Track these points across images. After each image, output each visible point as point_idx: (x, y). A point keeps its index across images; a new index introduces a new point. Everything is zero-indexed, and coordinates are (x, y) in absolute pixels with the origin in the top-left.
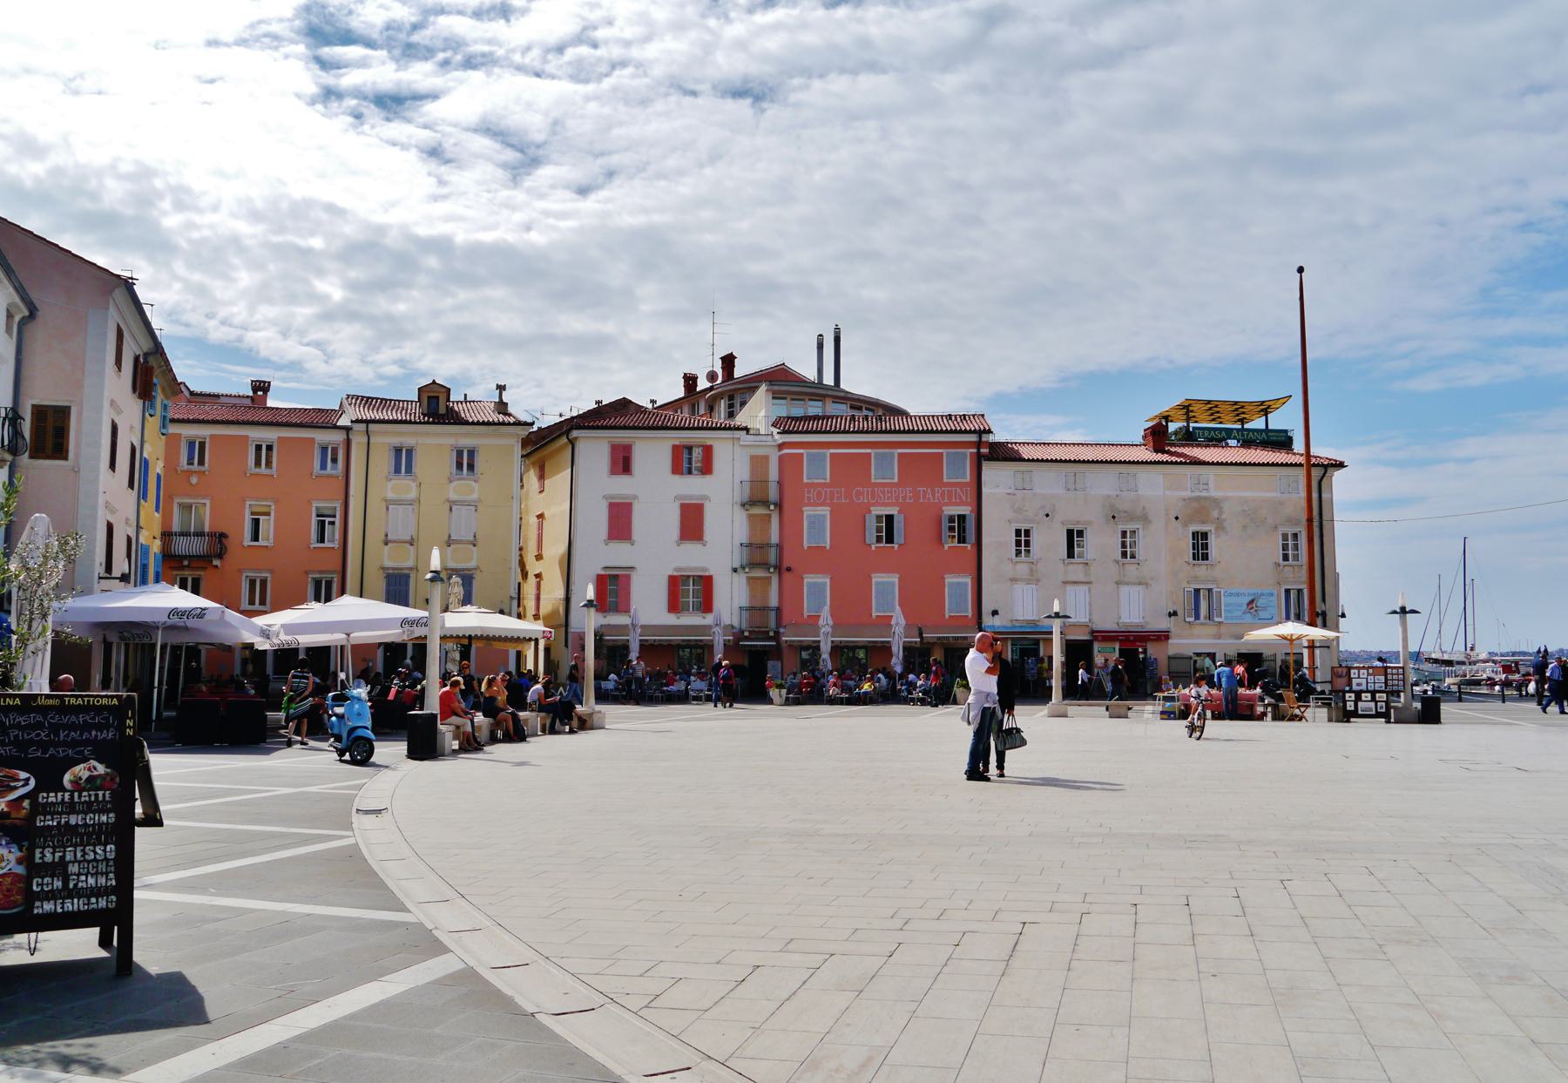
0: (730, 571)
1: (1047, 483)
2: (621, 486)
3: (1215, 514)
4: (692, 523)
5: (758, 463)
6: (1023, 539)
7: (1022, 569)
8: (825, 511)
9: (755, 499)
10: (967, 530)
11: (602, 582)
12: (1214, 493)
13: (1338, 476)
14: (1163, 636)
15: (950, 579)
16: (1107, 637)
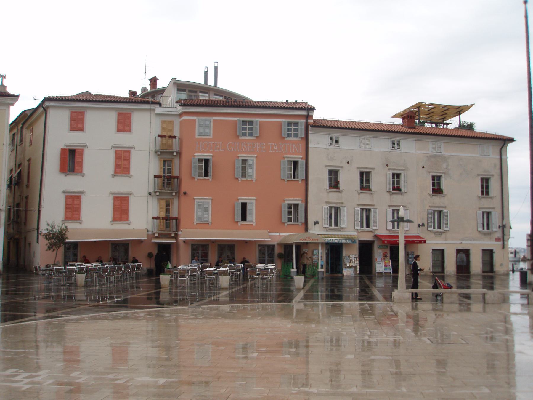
0: (146, 194)
1: (349, 143)
3: (444, 166)
4: (122, 162)
12: (444, 153)
13: (510, 146)
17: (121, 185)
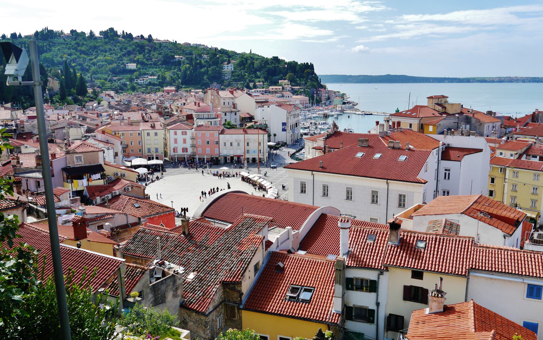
2: (176, 137)
4: (185, 141)
5: (193, 134)
6: (225, 144)
9: (193, 139)
10: (218, 143)
11: (174, 149)
14: (242, 156)
16: (235, 156)
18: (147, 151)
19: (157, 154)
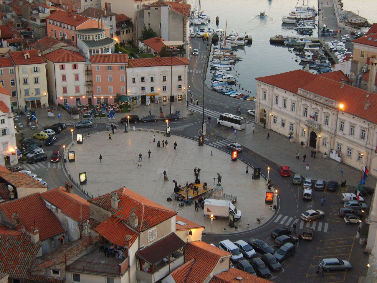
2: (63, 72)
4: (77, 78)
7: (134, 84)
8: (99, 76)
15: (122, 87)
17: (77, 83)
18: (23, 93)
19: (38, 96)
